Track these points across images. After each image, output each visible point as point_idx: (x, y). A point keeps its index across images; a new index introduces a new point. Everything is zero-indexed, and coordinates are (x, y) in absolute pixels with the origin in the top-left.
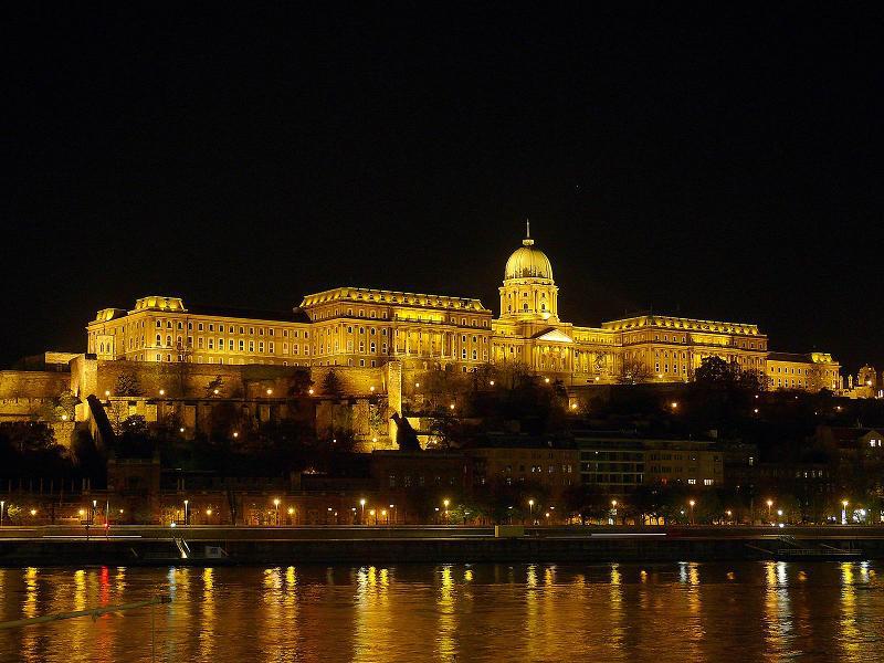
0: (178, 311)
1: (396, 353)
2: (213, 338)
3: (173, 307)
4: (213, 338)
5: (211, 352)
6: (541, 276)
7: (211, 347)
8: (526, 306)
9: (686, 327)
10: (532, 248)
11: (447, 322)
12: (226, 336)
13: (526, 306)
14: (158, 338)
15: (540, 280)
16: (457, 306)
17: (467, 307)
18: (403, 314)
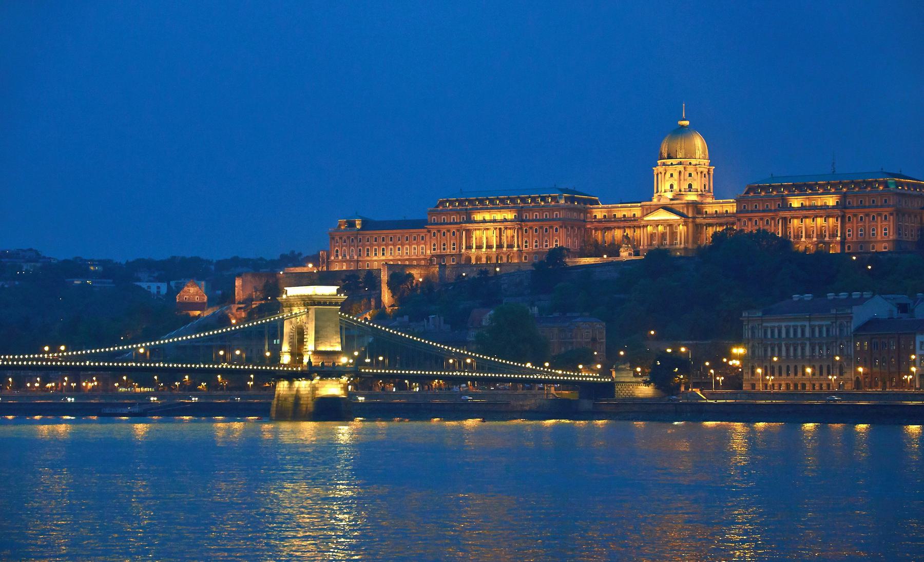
1: (463, 251)
7: (376, 255)
11: (519, 219)
14: (337, 251)
18: (478, 217)
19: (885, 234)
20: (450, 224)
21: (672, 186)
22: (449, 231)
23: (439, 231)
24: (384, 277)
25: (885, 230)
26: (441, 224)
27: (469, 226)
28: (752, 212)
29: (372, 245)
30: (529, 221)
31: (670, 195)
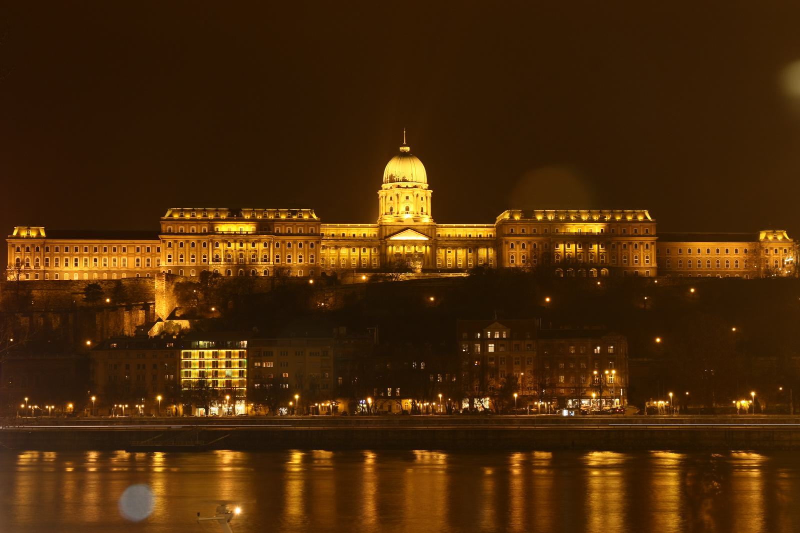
0: (39, 236)
1: (211, 263)
2: (68, 258)
3: (33, 234)
4: (68, 258)
5: (66, 269)
6: (404, 180)
7: (67, 265)
8: (391, 210)
9: (550, 217)
10: (404, 155)
12: (81, 255)
13: (391, 210)
15: (404, 184)
16: (283, 217)
17: (295, 217)
18: (223, 228)
19: (647, 262)
20: (190, 234)
21: (407, 209)
22: (187, 242)
23: (176, 241)
24: (159, 285)
25: (647, 257)
26: (178, 234)
27: (217, 238)
28: (520, 235)
29: (62, 255)
30: (281, 235)
31: (410, 216)
